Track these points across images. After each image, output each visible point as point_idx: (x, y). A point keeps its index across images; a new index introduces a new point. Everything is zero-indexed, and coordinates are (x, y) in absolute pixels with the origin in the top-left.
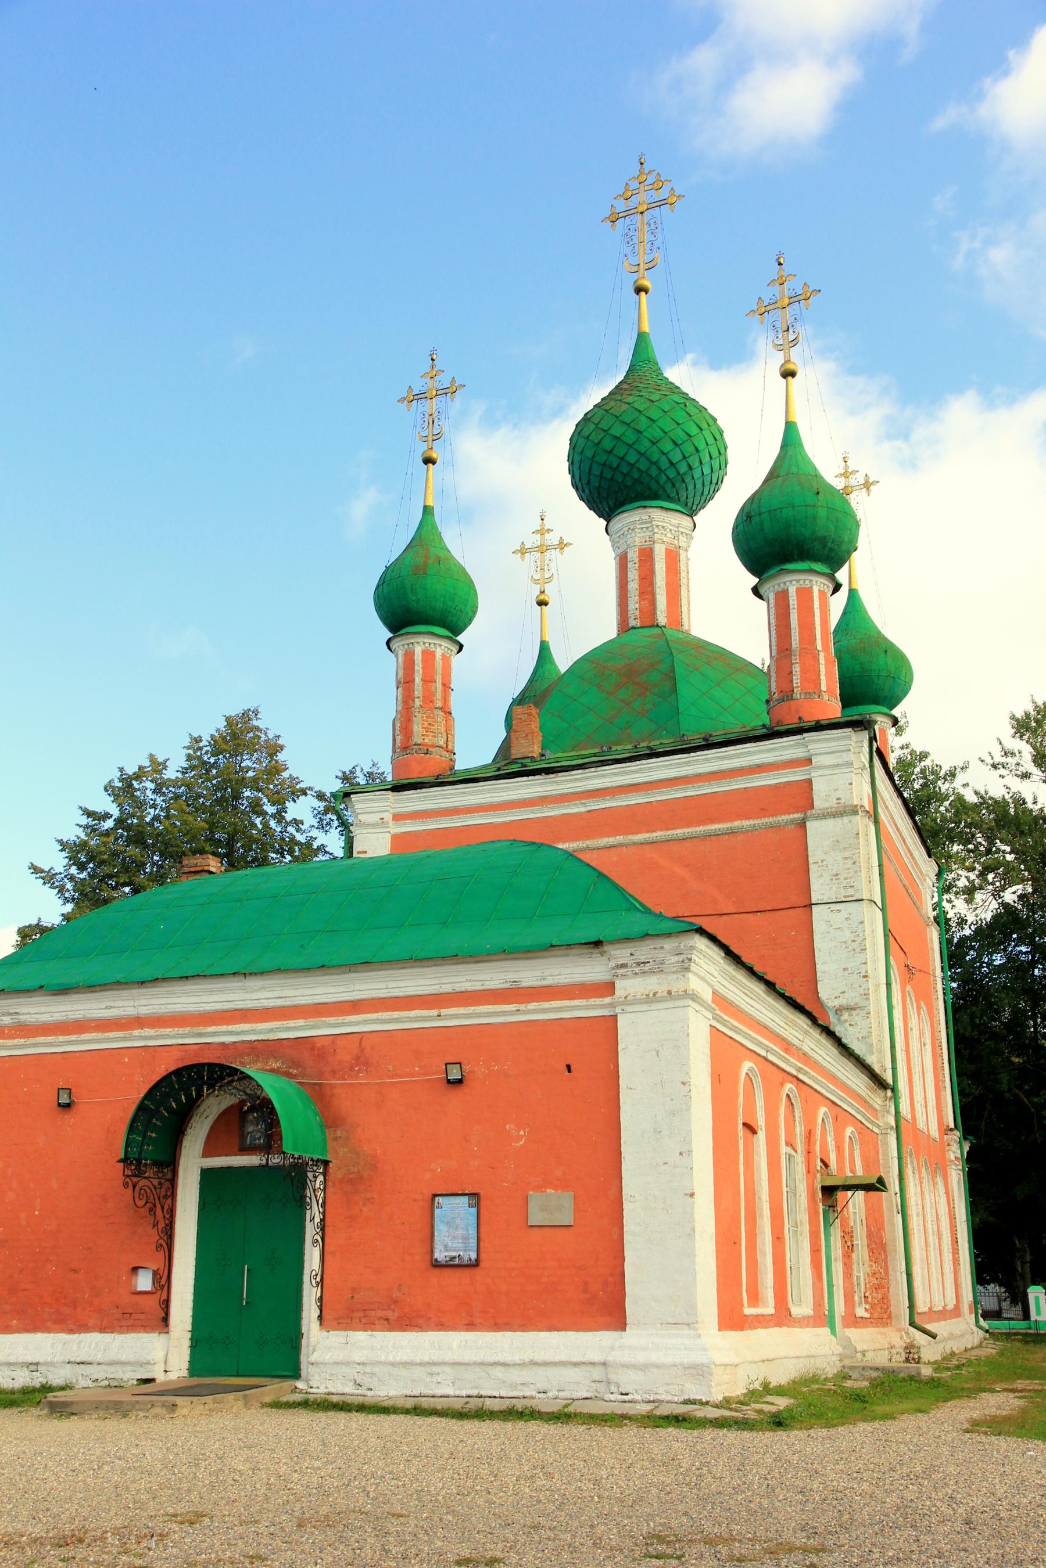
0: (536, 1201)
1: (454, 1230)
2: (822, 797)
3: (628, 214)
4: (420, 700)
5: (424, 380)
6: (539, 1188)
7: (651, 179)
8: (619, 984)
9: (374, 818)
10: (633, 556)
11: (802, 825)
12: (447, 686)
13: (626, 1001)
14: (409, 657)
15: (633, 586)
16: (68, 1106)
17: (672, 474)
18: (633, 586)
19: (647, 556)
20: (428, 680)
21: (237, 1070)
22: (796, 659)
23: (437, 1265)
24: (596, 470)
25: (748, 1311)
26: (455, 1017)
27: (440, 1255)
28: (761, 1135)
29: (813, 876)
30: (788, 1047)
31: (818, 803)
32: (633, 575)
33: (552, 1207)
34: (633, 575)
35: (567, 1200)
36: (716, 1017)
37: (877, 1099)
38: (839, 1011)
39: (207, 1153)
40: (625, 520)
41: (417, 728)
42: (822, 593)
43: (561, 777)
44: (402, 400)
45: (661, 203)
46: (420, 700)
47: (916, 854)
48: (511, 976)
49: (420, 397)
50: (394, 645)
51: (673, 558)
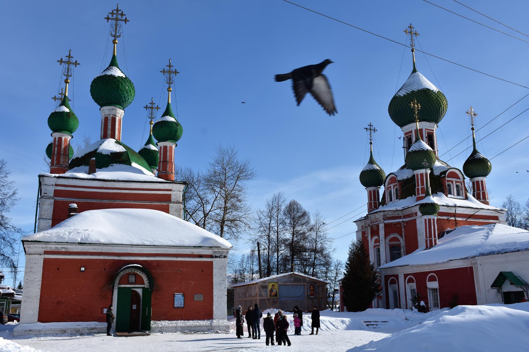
0: (196, 296)
2: (173, 198)
3: (112, 19)
5: (66, 58)
6: (196, 294)
7: (120, 12)
15: (109, 127)
17: (124, 100)
18: (109, 127)
23: (175, 308)
27: (175, 306)
31: (172, 200)
32: (110, 124)
33: (199, 298)
34: (110, 124)
35: (202, 296)
41: (62, 160)
44: (58, 61)
45: (122, 20)
49: (65, 62)
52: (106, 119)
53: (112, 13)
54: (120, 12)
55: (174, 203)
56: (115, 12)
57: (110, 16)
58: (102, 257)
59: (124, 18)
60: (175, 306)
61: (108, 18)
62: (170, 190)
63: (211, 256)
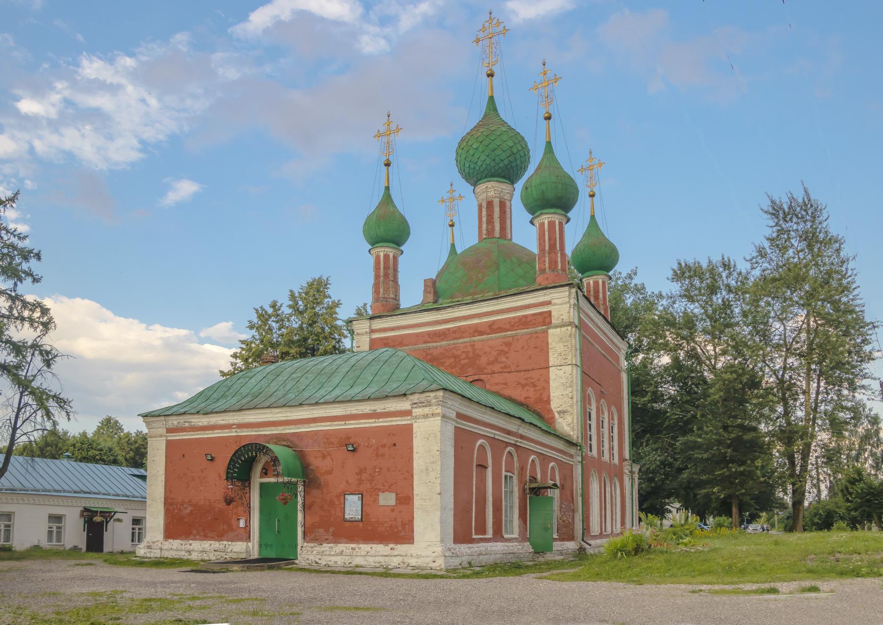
1: (353, 507)
4: (387, 276)
7: (495, 21)
8: (414, 410)
9: (364, 331)
10: (484, 205)
11: (545, 332)
12: (395, 270)
13: (416, 418)
14: (378, 257)
15: (484, 219)
16: (212, 459)
19: (490, 204)
20: (386, 268)
21: (264, 447)
22: (547, 255)
23: (345, 520)
24: (467, 165)
25: (474, 537)
26: (352, 425)
28: (490, 470)
29: (550, 354)
30: (509, 433)
32: (484, 213)
36: (457, 423)
37: (572, 451)
38: (559, 412)
39: (261, 477)
40: (481, 187)
42: (561, 224)
43: (442, 312)
46: (387, 276)
47: (615, 340)
48: (373, 408)
50: (372, 252)
51: (502, 205)
52: (480, 206)
53: (484, 29)
54: (495, 21)
55: (556, 327)
56: (487, 24)
57: (481, 35)
58: (233, 433)
59: (501, 28)
60: (347, 516)
61: (478, 41)
62: (549, 303)
63: (408, 413)
